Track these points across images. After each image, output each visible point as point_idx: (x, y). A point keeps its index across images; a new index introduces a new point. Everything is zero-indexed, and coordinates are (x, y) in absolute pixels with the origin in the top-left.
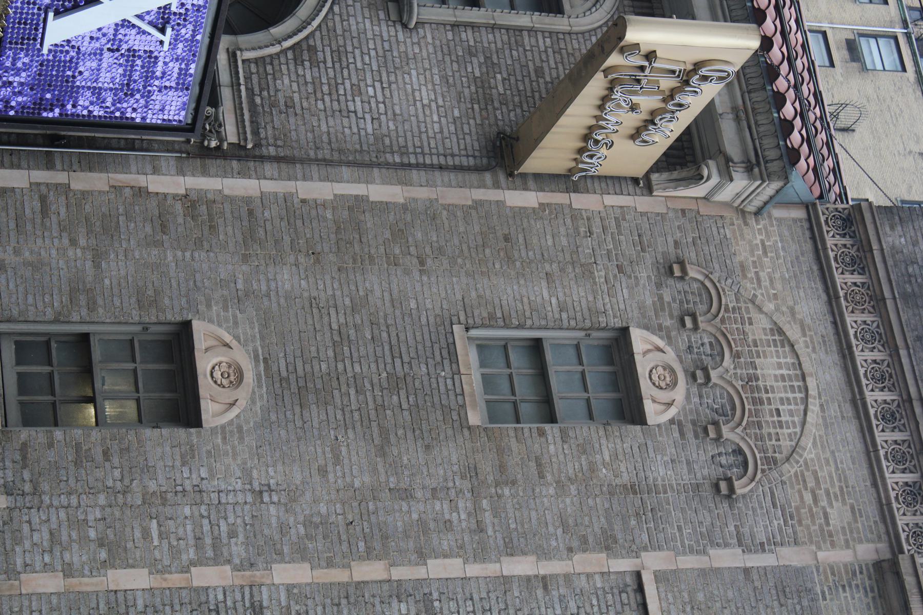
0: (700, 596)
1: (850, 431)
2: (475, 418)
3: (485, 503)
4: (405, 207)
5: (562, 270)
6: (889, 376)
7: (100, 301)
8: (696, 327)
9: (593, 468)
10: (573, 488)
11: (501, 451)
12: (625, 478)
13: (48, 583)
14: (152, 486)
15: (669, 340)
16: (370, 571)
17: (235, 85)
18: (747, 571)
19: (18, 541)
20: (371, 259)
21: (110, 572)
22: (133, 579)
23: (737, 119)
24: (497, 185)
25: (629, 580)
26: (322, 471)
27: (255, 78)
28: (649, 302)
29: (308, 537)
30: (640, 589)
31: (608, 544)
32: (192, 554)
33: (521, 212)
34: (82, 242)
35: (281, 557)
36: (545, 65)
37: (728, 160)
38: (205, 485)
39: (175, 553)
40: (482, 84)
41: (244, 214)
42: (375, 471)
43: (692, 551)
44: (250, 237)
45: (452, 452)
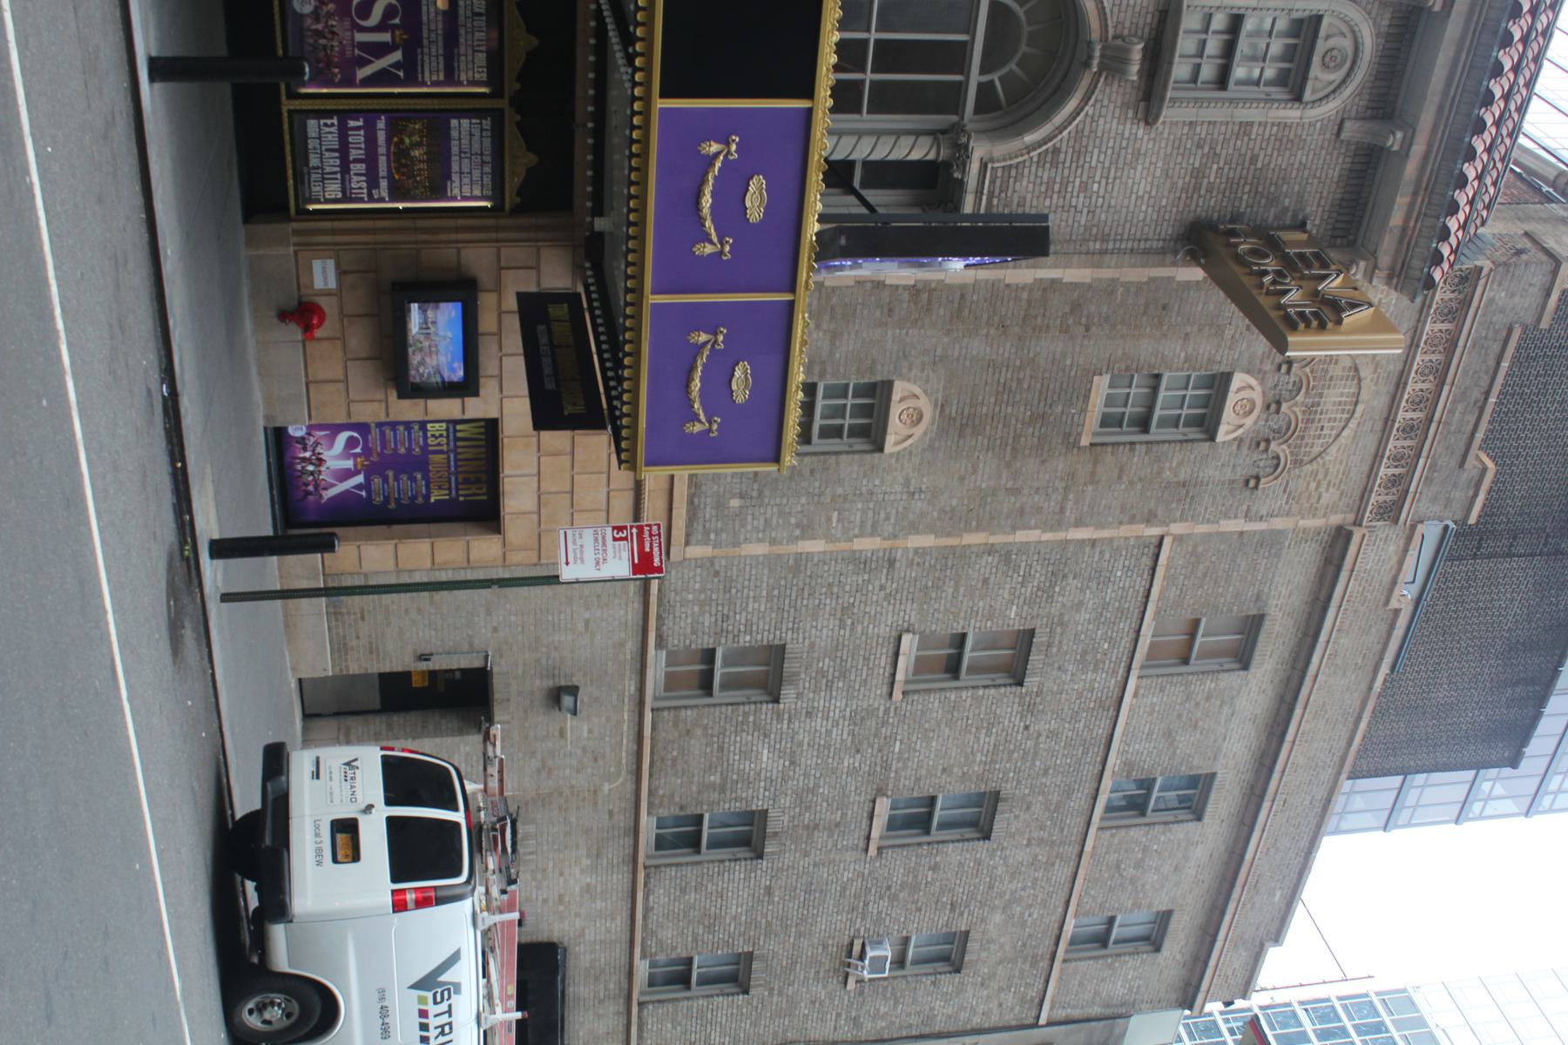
0: (1200, 549)
1: (1370, 442)
2: (1085, 441)
3: (1071, 496)
4: (1089, 286)
5: (1200, 330)
6: (1427, 403)
7: (829, 370)
8: (1288, 372)
9: (1159, 473)
10: (1139, 486)
11: (1096, 463)
12: (1182, 477)
13: (760, 549)
14: (840, 491)
15: (1262, 382)
16: (976, 539)
17: (979, 192)
18: (1241, 533)
19: (743, 525)
20: (1048, 328)
21: (800, 543)
22: (815, 546)
24: (1174, 264)
25: (1155, 541)
26: (962, 479)
27: (998, 181)
28: (1260, 353)
29: (939, 519)
30: (1160, 545)
31: (1150, 519)
32: (857, 531)
33: (1187, 285)
34: (825, 327)
35: (917, 531)
36: (1262, 153)
38: (876, 490)
39: (846, 530)
40: (1198, 174)
41: (957, 297)
42: (1000, 476)
43: (1208, 521)
44: (958, 314)
45: (1060, 465)
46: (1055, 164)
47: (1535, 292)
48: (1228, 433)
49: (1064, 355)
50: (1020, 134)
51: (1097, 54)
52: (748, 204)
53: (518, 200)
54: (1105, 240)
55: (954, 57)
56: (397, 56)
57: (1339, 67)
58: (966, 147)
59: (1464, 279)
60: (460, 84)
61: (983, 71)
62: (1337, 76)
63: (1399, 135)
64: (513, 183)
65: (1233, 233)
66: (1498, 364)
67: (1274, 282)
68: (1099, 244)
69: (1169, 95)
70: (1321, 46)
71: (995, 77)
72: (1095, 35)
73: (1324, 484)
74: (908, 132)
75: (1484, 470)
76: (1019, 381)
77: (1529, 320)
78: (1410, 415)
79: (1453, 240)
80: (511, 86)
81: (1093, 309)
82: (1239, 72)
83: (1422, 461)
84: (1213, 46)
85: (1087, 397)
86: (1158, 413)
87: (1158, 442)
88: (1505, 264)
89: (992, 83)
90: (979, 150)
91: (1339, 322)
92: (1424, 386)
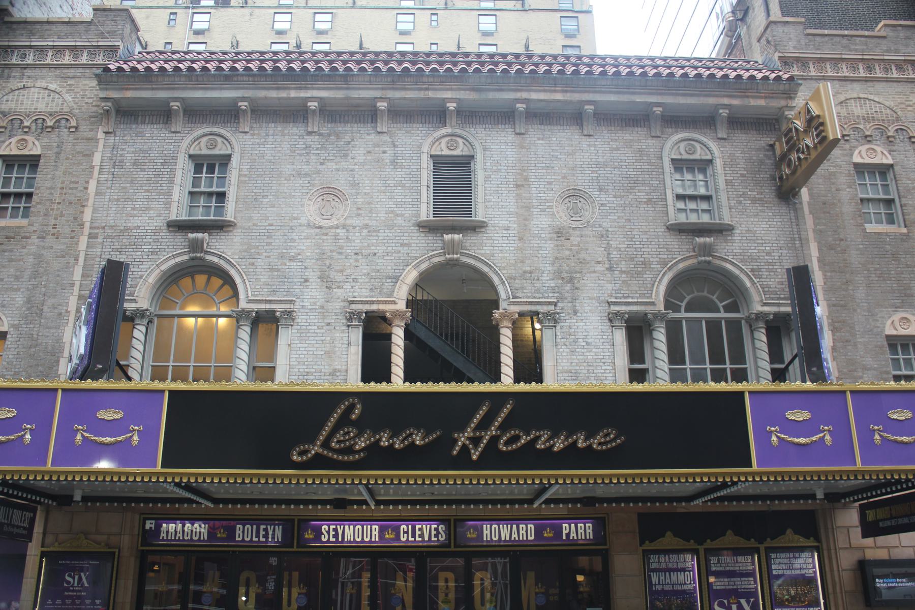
1: (879, 86)
2: (904, 230)
4: (819, 243)
8: (848, 135)
15: (856, 147)
17: (779, 305)
20: (845, 260)
23: (770, 97)
24: (801, 203)
34: (860, 374)
37: (787, 106)
40: (754, 201)
41: (835, 308)
46: (759, 270)
47: (786, 29)
48: (887, 158)
49: (858, 249)
50: (747, 289)
51: (703, 258)
52: (801, 419)
53: (812, 539)
54: (793, 239)
55: (714, 327)
56: (743, 601)
57: (694, 146)
58: (757, 314)
59: (786, 63)
60: (754, 570)
61: (719, 312)
62: (697, 145)
63: (721, 111)
64: (803, 542)
65: (781, 178)
66: (826, 35)
67: (803, 153)
68: (797, 242)
69: (718, 221)
70: (685, 156)
71: (720, 305)
72: (695, 261)
73: (907, 103)
74: (753, 344)
75: (885, 25)
76: (876, 270)
77: (801, 27)
78: (861, 70)
79: (767, 74)
80: (753, 543)
81: (831, 239)
82: (702, 191)
83: (886, 58)
84: (692, 205)
85: (879, 234)
86: (882, 196)
87: (898, 193)
88: (775, 46)
89: (723, 307)
90: (758, 308)
91: (818, 116)
92: (844, 67)
